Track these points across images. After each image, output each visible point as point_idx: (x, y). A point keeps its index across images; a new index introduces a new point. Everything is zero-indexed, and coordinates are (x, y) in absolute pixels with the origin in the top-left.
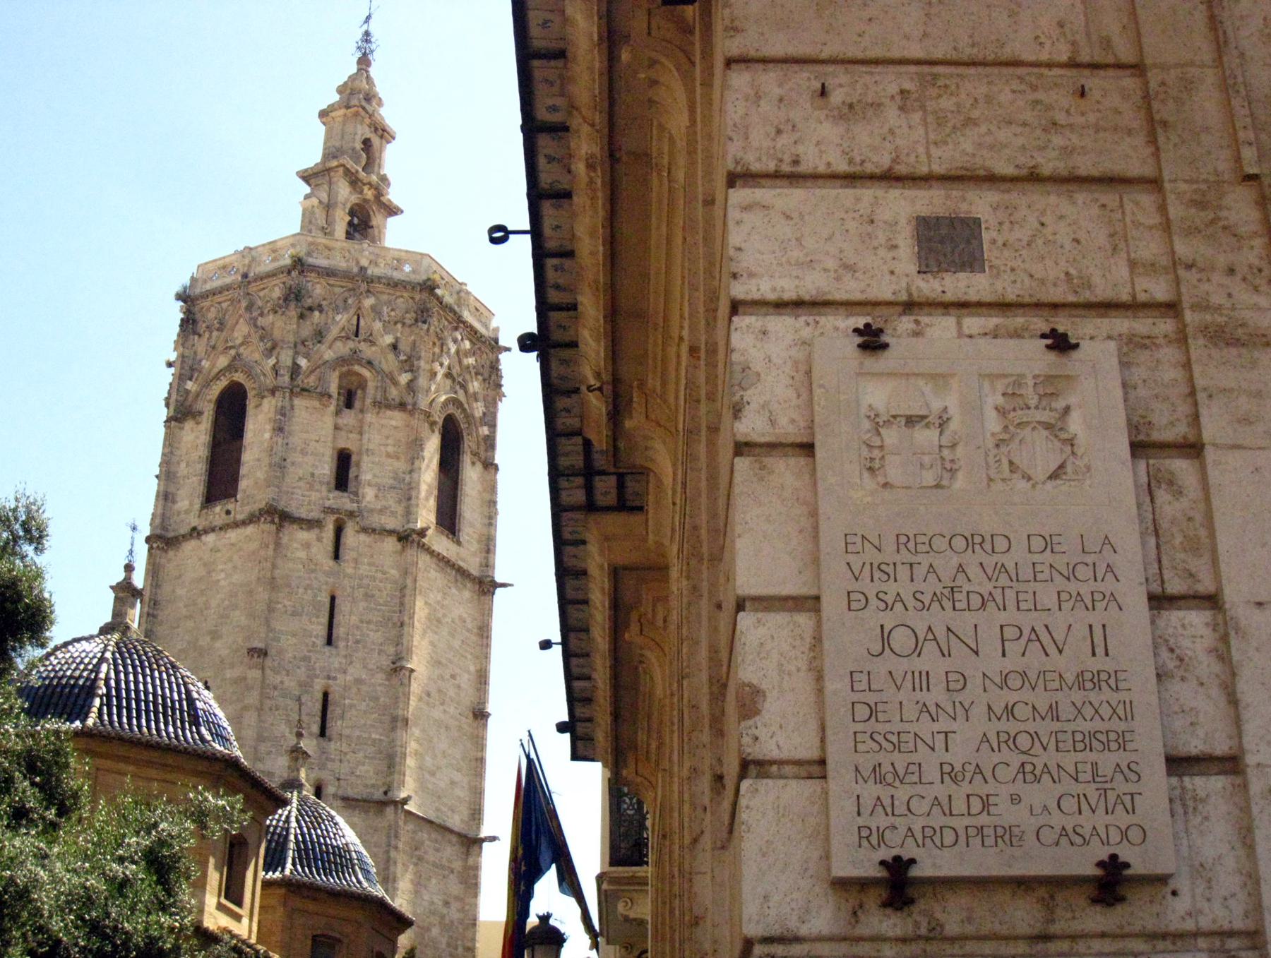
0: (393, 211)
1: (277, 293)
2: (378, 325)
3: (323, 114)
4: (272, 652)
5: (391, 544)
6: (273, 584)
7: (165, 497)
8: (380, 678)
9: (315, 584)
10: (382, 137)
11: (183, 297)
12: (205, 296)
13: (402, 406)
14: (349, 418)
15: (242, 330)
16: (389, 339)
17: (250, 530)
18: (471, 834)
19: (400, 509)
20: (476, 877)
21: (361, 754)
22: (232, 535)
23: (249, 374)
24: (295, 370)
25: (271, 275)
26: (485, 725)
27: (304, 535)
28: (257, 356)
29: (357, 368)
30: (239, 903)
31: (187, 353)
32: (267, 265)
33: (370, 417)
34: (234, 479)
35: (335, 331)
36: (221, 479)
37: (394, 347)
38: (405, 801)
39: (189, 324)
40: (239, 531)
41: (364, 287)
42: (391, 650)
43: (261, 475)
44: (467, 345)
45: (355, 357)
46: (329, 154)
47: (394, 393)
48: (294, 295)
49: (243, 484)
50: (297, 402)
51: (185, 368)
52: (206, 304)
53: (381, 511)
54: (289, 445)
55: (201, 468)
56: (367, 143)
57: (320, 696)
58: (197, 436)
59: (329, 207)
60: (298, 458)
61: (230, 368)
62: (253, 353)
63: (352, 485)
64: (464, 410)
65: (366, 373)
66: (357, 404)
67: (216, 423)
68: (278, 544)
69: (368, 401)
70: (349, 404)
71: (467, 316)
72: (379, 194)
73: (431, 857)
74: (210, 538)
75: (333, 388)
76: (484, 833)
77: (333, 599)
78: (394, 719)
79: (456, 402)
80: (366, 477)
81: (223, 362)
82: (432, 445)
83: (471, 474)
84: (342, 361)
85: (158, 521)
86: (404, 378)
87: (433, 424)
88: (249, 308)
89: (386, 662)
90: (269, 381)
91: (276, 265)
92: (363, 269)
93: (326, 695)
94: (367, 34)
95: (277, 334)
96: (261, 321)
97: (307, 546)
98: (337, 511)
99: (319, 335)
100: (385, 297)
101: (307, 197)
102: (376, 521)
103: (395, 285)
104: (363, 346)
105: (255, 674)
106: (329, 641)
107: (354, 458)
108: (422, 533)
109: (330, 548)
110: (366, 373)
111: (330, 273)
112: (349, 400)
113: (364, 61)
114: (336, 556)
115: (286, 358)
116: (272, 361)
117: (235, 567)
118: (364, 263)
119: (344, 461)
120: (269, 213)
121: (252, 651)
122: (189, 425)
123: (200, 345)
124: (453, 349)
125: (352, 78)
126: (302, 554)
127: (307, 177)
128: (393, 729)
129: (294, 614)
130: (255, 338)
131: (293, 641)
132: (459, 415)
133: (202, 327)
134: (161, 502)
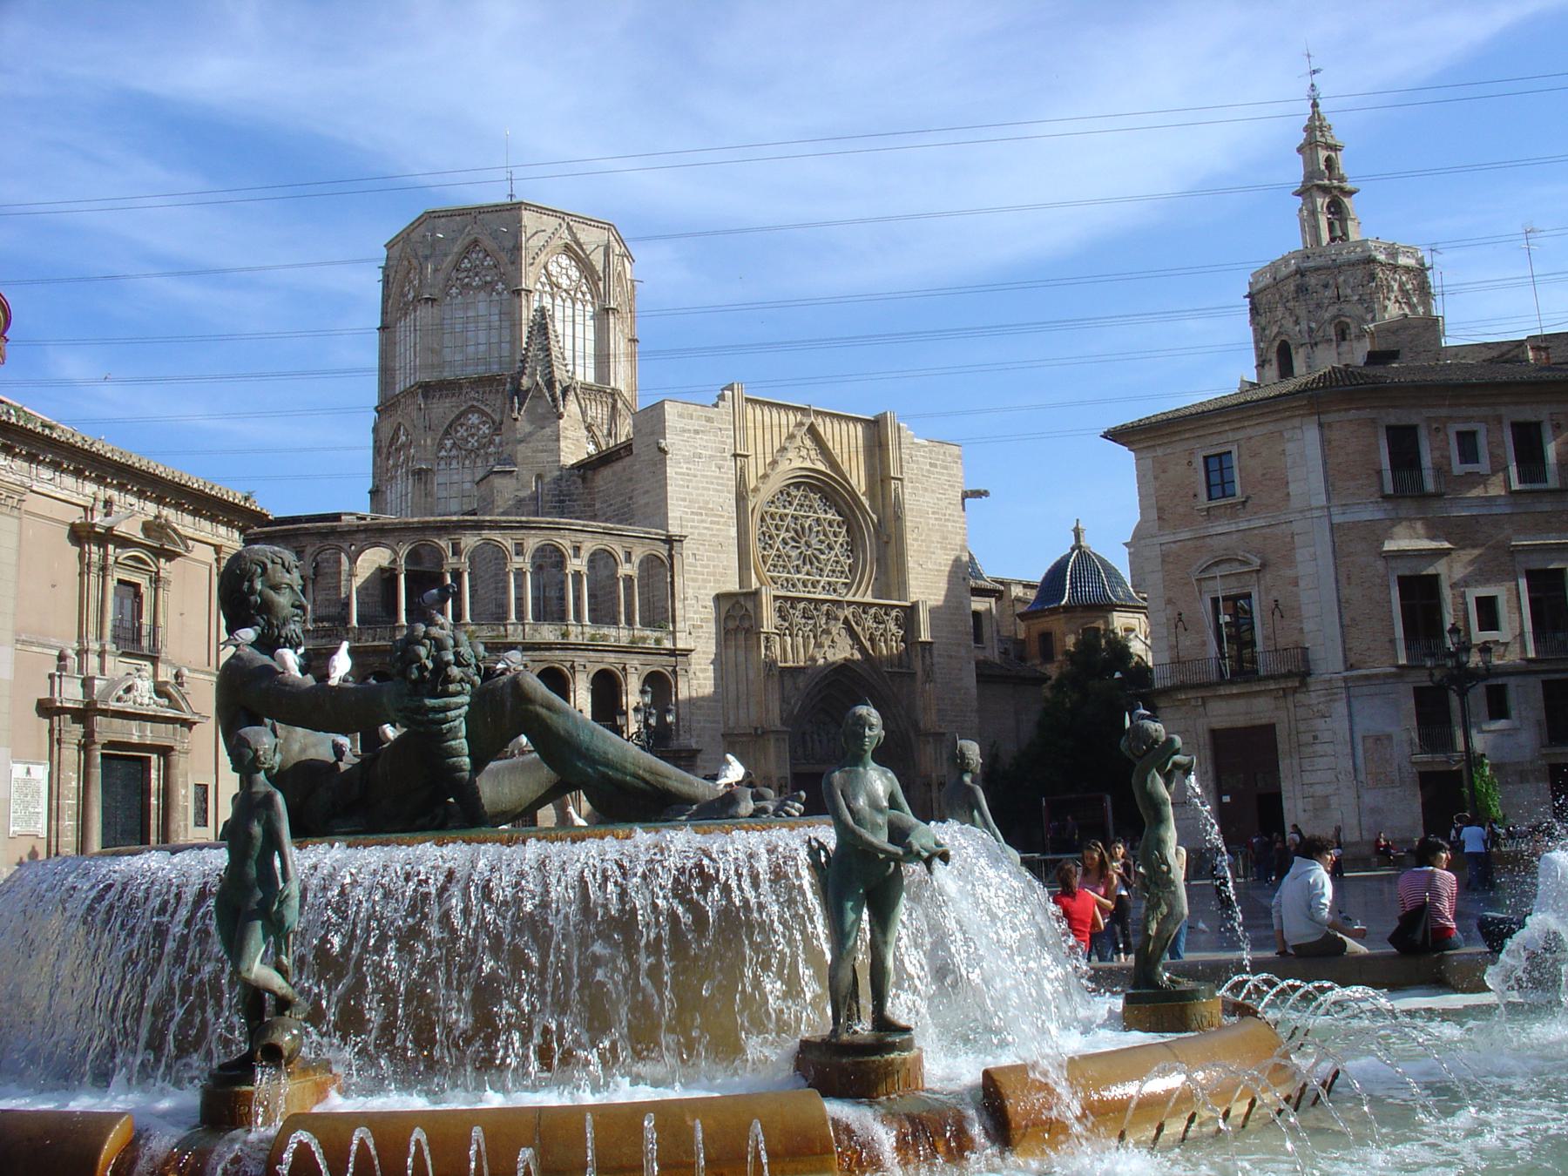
2: (1349, 291)
3: (1299, 150)
11: (1250, 296)
12: (1260, 291)
14: (1345, 346)
24: (1311, 330)
25: (1287, 277)
32: (1284, 271)
33: (1355, 344)
39: (1255, 311)
48: (1302, 290)
56: (1328, 159)
59: (1313, 213)
61: (1279, 333)
81: (1275, 329)
103: (1352, 264)
111: (1317, 269)
113: (1315, 105)
115: (1304, 326)
120: (1282, 237)
124: (1396, 287)
125: (1311, 119)
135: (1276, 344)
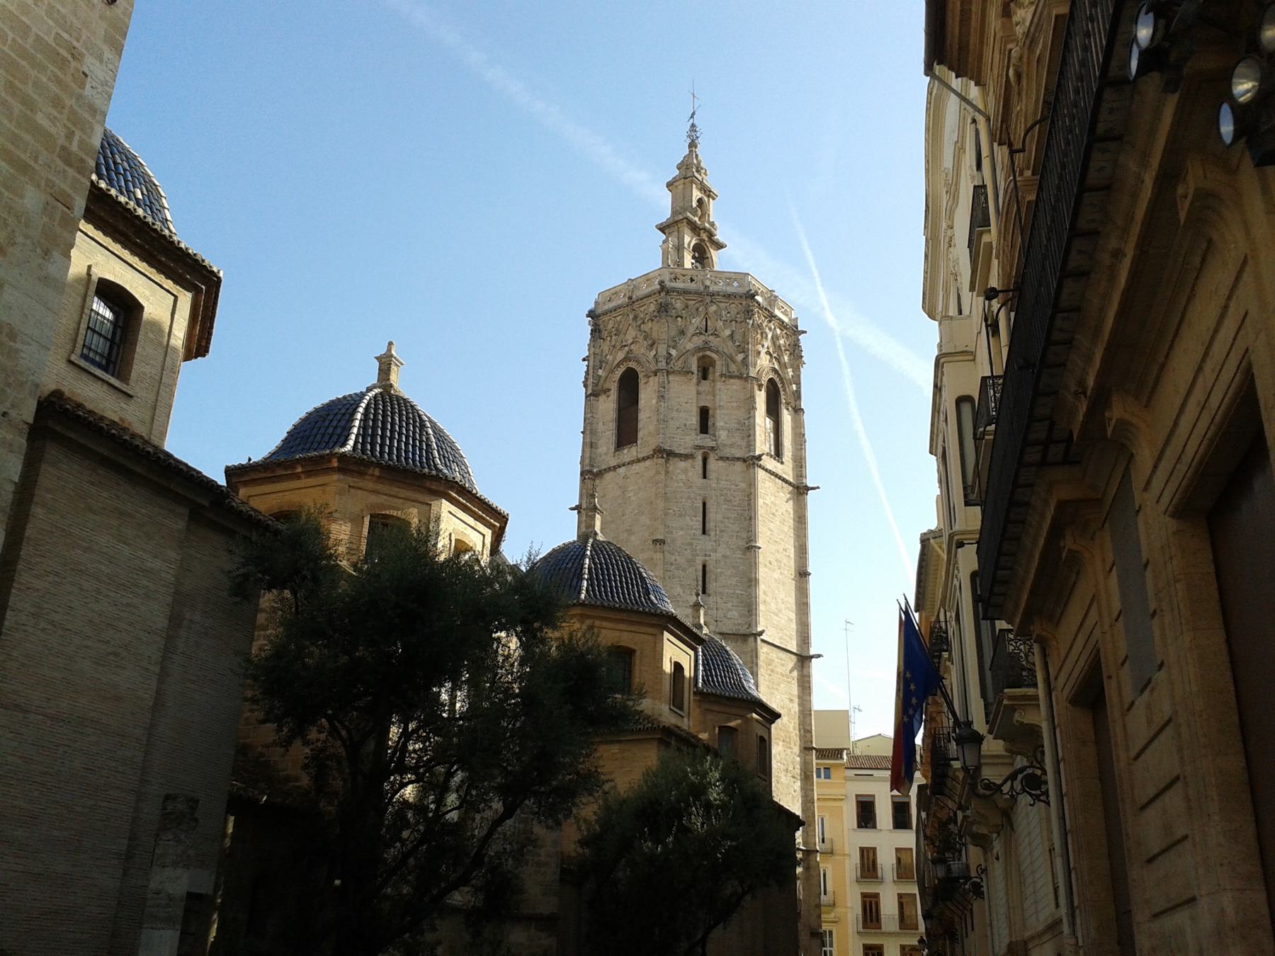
0: (720, 246)
1: (652, 308)
3: (669, 185)
4: (668, 540)
5: (739, 466)
6: (666, 499)
7: (590, 444)
8: (739, 554)
9: (692, 495)
10: (709, 196)
11: (591, 314)
12: (605, 313)
13: (740, 377)
14: (705, 385)
15: (631, 334)
16: (728, 332)
17: (648, 463)
18: (805, 654)
19: (744, 444)
20: (809, 682)
21: (729, 605)
22: (636, 467)
23: (638, 362)
25: (649, 296)
26: (807, 582)
27: (682, 464)
28: (643, 350)
29: (708, 353)
30: (682, 709)
31: (598, 351)
32: (644, 290)
34: (635, 431)
35: (691, 330)
36: (626, 433)
37: (732, 336)
38: (761, 633)
39: (596, 332)
40: (641, 464)
41: (708, 299)
42: (745, 535)
43: (652, 428)
44: (778, 331)
45: (706, 346)
46: (674, 212)
47: (733, 368)
48: (664, 309)
49: (640, 434)
50: (671, 378)
51: (595, 361)
52: (606, 318)
53: (732, 446)
54: (668, 407)
55: (612, 426)
56: (700, 201)
57: (700, 568)
58: (608, 406)
59: (679, 248)
60: (675, 414)
61: (626, 359)
62: (640, 349)
63: (710, 431)
64: (779, 375)
65: (713, 355)
66: (710, 377)
67: (619, 395)
68: (667, 472)
69: (718, 374)
70: (705, 377)
71: (777, 313)
72: (711, 235)
73: (779, 670)
74: (622, 470)
75: (694, 368)
76: (812, 653)
77: (704, 504)
78: (750, 580)
79: (774, 370)
80: (720, 424)
81: (621, 355)
82: (761, 398)
83: (787, 417)
84: (699, 349)
85: (587, 461)
86: (740, 357)
87: (760, 387)
88: (635, 318)
89: (742, 543)
90: (653, 367)
91: (650, 289)
92: (707, 287)
93: (704, 567)
94: (693, 125)
95: (655, 335)
96: (646, 327)
97: (685, 471)
98: (703, 447)
99: (682, 333)
100: (722, 305)
101: (664, 242)
102: (728, 452)
103: (728, 296)
104: (711, 338)
105: (659, 556)
106: (704, 533)
107: (711, 412)
108: (759, 458)
109: (701, 472)
110: (713, 355)
111: (685, 292)
112: (704, 373)
113: (693, 145)
114: (705, 477)
115: (662, 350)
116: (653, 353)
117: (640, 489)
118: (708, 283)
119: (704, 414)
120: (640, 257)
121: (655, 541)
122: (602, 398)
123: (606, 347)
124: (770, 336)
126: (683, 477)
127: (662, 228)
128: (750, 586)
129: (681, 515)
130: (640, 339)
131: (681, 533)
132: (775, 377)
133: (605, 334)
134: (588, 450)
135: (622, 369)
